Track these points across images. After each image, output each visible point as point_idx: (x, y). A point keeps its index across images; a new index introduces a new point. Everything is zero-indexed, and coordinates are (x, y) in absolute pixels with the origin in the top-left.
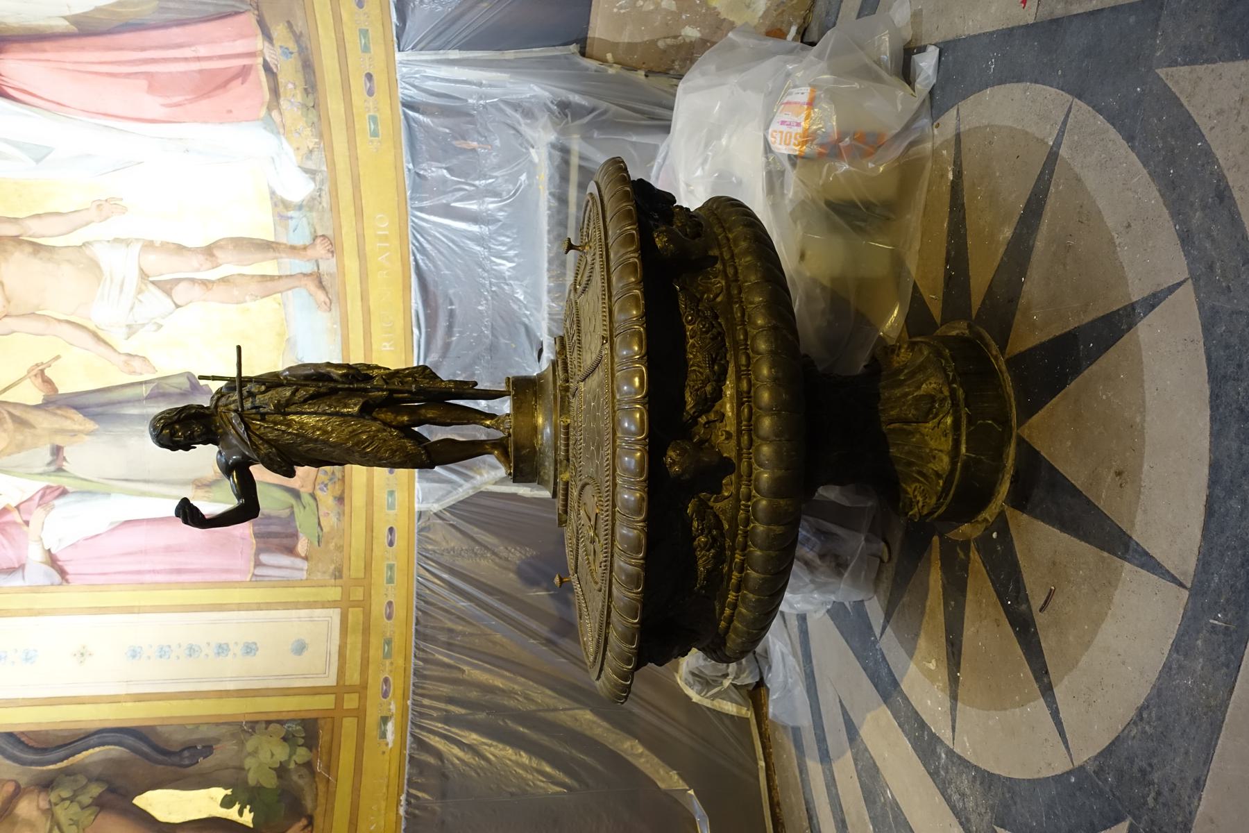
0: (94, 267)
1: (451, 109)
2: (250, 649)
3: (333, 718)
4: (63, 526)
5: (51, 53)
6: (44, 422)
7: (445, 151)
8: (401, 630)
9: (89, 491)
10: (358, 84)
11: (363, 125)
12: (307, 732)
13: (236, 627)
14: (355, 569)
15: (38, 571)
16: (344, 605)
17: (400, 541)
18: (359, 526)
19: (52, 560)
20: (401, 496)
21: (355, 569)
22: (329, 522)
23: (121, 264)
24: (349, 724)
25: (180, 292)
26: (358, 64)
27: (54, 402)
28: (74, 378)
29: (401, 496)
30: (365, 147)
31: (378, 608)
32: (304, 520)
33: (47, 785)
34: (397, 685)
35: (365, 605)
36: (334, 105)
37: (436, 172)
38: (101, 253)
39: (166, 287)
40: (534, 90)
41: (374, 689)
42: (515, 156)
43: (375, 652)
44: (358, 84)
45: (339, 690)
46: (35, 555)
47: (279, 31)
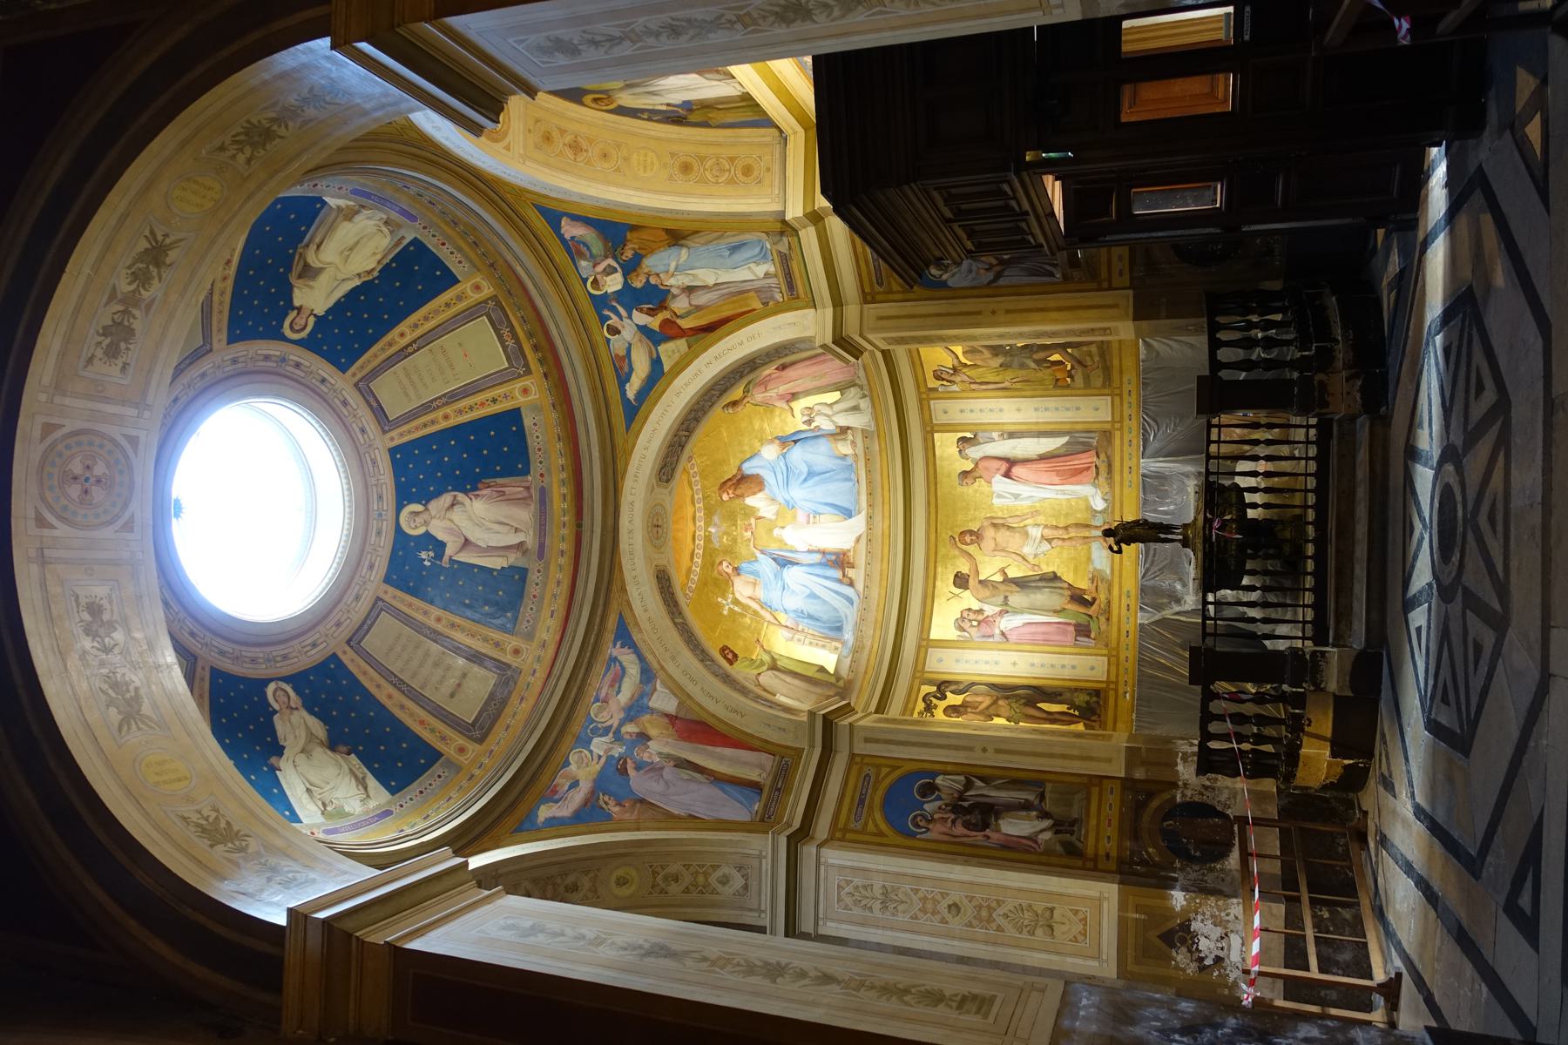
0: (1027, 534)
1: (1161, 477)
2: (1074, 667)
3: (1106, 691)
4: (1008, 623)
5: (1029, 465)
6: (1002, 587)
7: (1156, 490)
8: (1131, 666)
9: (1017, 612)
10: (1126, 470)
11: (1126, 483)
12: (1097, 693)
13: (1068, 660)
14: (1114, 644)
15: (998, 638)
16: (1109, 656)
17: (1131, 636)
18: (1115, 629)
19: (1003, 634)
20: (1132, 620)
21: (1114, 644)
22: (1103, 627)
23: (1036, 532)
24: (1112, 693)
25: (1054, 543)
26: (1126, 464)
27: (1007, 581)
28: (1013, 573)
29: (1132, 620)
30: (1126, 491)
31: (1122, 658)
32: (1093, 626)
33: (1007, 698)
34: (1130, 682)
35: (1117, 656)
36: (1117, 478)
37: (1151, 497)
38: (1030, 529)
39: (1049, 541)
40: (1189, 468)
41: (1121, 682)
42: (1182, 490)
43: (1122, 671)
44: (1126, 470)
45: (1108, 682)
46: (997, 631)
47: (1102, 456)
